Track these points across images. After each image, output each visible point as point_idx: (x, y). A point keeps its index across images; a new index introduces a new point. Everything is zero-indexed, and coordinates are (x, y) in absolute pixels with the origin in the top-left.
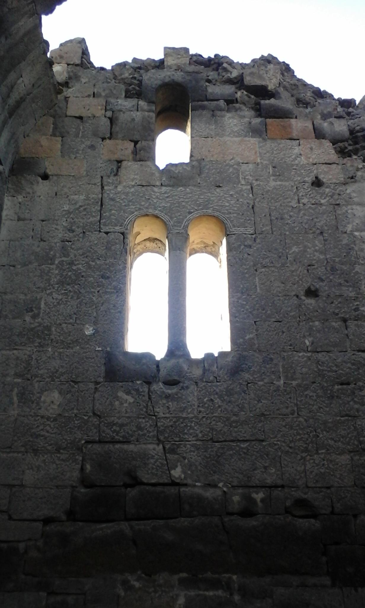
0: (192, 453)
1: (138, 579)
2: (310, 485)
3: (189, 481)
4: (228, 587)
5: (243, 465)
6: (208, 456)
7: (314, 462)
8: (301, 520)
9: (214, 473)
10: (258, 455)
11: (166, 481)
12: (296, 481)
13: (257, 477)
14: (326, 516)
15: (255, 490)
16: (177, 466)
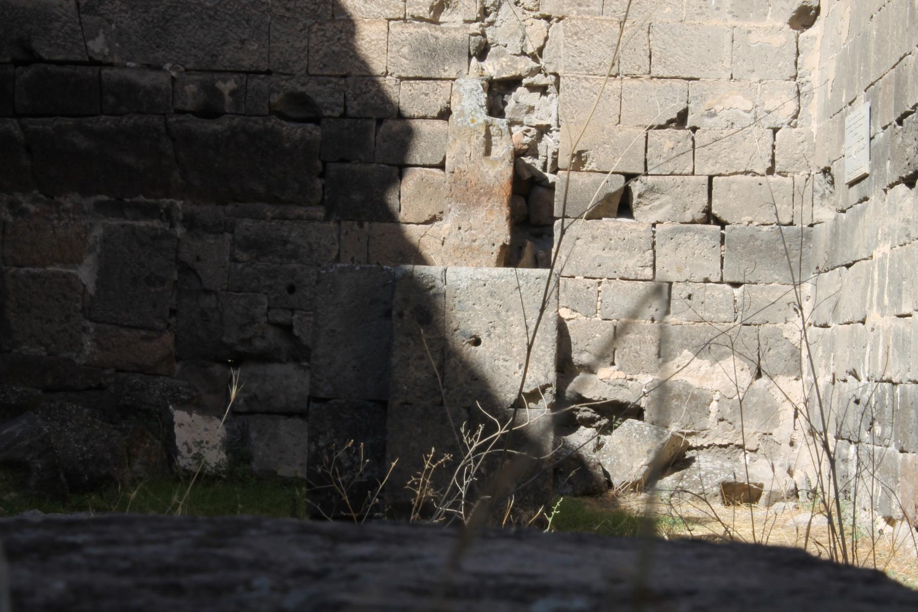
0: (123, 14)
1: (35, 201)
2: (312, 72)
3: (116, 59)
4: (168, 215)
5: (206, 36)
6: (150, 19)
7: (324, 35)
8: (292, 125)
9: (158, 47)
10: (233, 20)
11: (79, 58)
12: (290, 64)
13: (227, 57)
14: (331, 120)
15: (222, 76)
16: (97, 35)
